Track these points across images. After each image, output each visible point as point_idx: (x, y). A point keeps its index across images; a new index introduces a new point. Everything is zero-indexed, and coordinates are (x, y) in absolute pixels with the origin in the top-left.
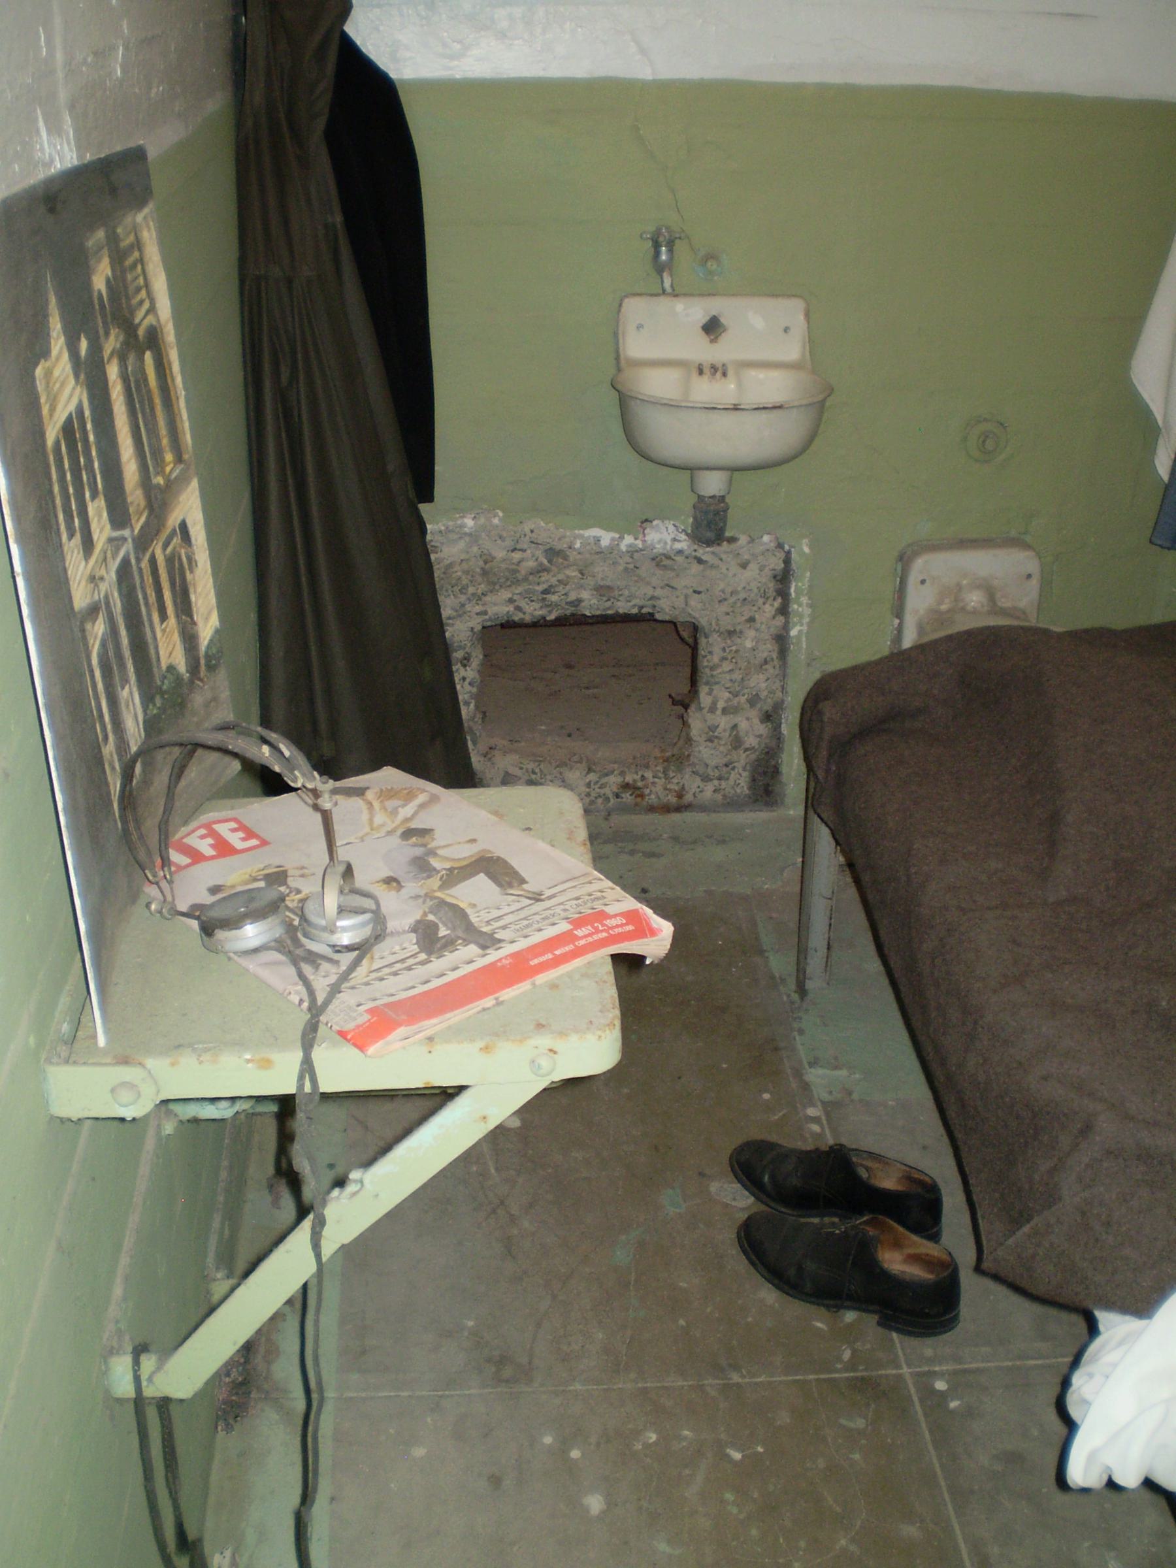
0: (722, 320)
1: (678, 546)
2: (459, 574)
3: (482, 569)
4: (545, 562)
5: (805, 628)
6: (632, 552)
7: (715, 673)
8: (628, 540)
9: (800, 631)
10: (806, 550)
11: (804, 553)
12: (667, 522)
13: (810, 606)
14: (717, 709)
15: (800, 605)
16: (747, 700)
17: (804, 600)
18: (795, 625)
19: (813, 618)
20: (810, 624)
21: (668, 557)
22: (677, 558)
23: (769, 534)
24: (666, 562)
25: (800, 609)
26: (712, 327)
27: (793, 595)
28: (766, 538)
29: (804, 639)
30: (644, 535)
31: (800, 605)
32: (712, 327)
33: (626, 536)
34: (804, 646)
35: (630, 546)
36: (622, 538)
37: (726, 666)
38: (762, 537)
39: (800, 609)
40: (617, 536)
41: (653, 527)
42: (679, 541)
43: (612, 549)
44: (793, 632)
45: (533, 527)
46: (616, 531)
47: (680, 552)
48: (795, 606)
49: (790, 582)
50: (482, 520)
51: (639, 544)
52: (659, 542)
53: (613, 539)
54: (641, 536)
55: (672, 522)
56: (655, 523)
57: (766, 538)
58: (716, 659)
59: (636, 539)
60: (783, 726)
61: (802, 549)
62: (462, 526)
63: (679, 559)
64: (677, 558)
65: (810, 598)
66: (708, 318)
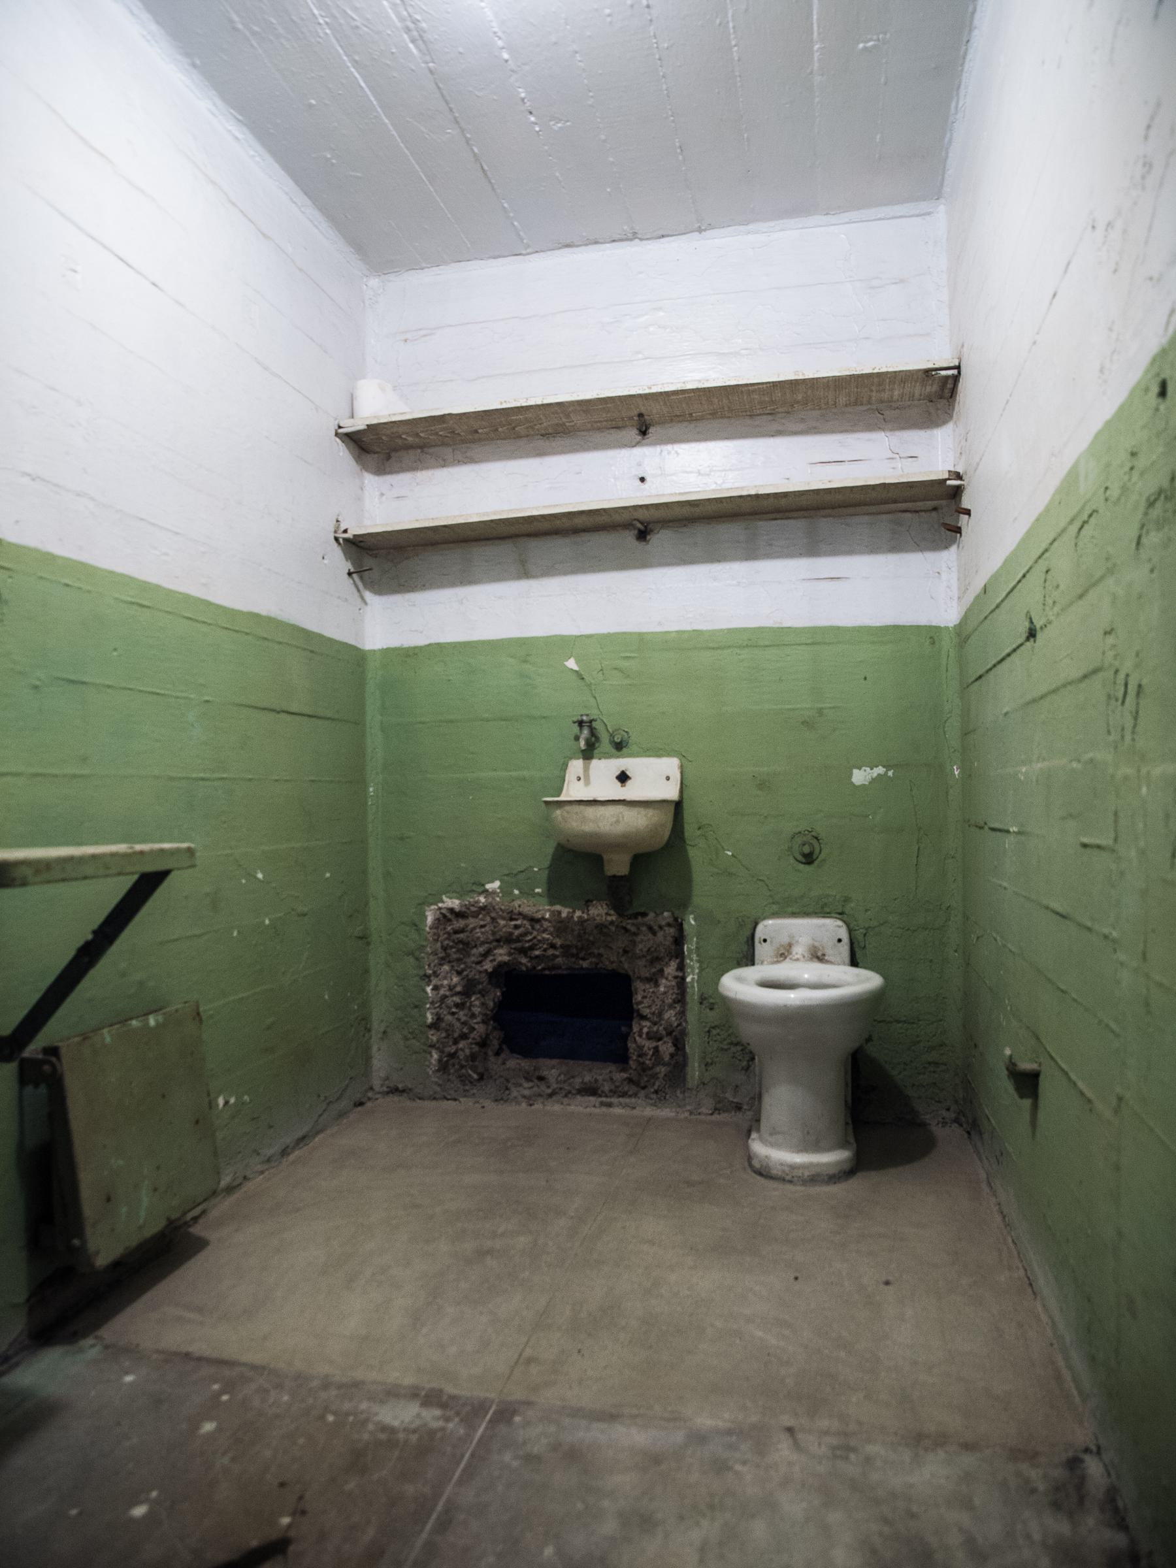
0: (628, 773)
1: (609, 918)
2: (479, 934)
3: (492, 931)
4: (530, 927)
5: (696, 977)
6: (582, 922)
7: (640, 1007)
8: (578, 913)
9: (693, 979)
10: (693, 922)
11: (692, 925)
12: (602, 902)
13: (698, 961)
14: (643, 1033)
15: (692, 960)
16: (664, 1028)
17: (695, 957)
18: (689, 975)
19: (701, 969)
20: (699, 974)
21: (606, 927)
22: (610, 927)
23: (667, 911)
24: (605, 930)
25: (692, 963)
26: (623, 778)
27: (686, 953)
28: (666, 914)
29: (696, 985)
30: (588, 911)
31: (692, 960)
32: (623, 778)
33: (577, 911)
34: (696, 989)
35: (580, 917)
36: (574, 912)
37: (646, 1002)
38: (663, 913)
39: (692, 963)
40: (571, 910)
41: (593, 906)
42: (610, 915)
43: (570, 917)
44: (688, 979)
45: (519, 903)
46: (570, 907)
47: (612, 923)
48: (688, 961)
49: (683, 945)
50: (490, 900)
51: (585, 916)
52: (598, 915)
53: (569, 913)
54: (586, 911)
55: (605, 902)
56: (594, 902)
57: (666, 914)
58: (639, 998)
59: (583, 913)
60: (687, 1046)
61: (690, 922)
62: (478, 902)
63: (613, 929)
64: (610, 927)
65: (698, 956)
66: (619, 772)
